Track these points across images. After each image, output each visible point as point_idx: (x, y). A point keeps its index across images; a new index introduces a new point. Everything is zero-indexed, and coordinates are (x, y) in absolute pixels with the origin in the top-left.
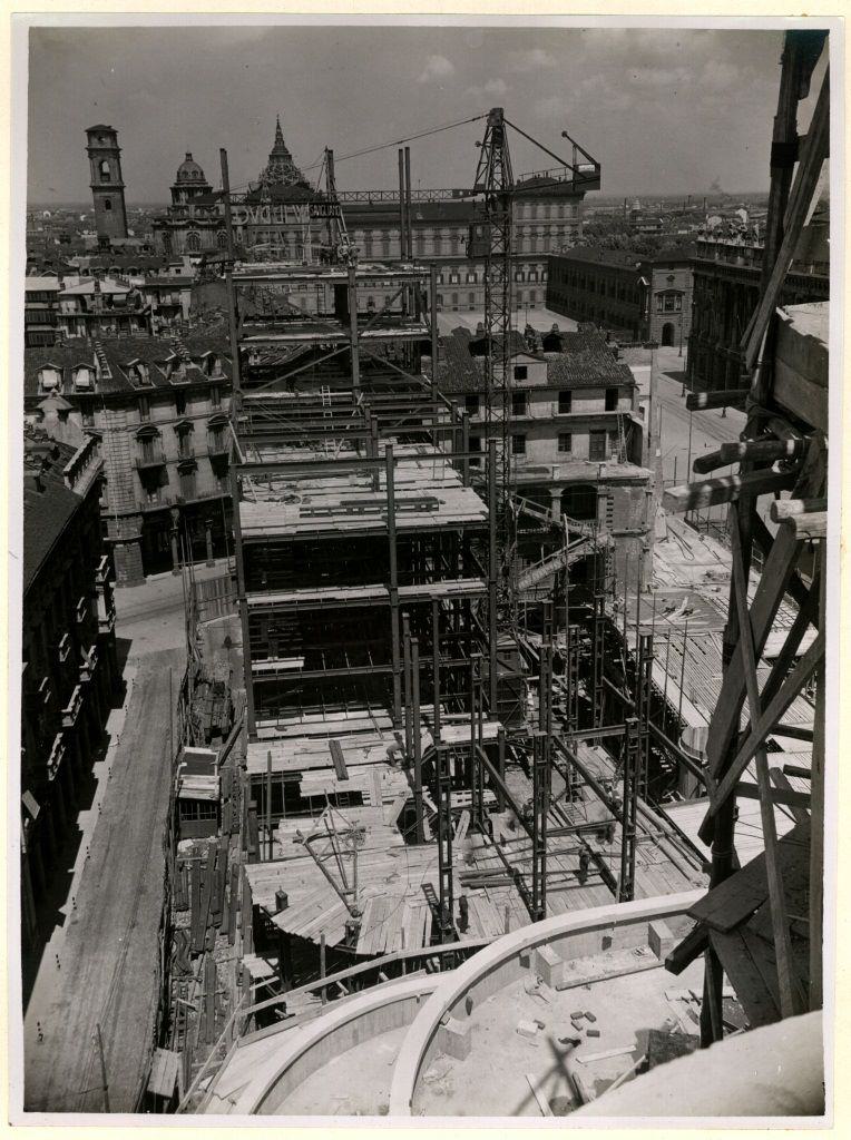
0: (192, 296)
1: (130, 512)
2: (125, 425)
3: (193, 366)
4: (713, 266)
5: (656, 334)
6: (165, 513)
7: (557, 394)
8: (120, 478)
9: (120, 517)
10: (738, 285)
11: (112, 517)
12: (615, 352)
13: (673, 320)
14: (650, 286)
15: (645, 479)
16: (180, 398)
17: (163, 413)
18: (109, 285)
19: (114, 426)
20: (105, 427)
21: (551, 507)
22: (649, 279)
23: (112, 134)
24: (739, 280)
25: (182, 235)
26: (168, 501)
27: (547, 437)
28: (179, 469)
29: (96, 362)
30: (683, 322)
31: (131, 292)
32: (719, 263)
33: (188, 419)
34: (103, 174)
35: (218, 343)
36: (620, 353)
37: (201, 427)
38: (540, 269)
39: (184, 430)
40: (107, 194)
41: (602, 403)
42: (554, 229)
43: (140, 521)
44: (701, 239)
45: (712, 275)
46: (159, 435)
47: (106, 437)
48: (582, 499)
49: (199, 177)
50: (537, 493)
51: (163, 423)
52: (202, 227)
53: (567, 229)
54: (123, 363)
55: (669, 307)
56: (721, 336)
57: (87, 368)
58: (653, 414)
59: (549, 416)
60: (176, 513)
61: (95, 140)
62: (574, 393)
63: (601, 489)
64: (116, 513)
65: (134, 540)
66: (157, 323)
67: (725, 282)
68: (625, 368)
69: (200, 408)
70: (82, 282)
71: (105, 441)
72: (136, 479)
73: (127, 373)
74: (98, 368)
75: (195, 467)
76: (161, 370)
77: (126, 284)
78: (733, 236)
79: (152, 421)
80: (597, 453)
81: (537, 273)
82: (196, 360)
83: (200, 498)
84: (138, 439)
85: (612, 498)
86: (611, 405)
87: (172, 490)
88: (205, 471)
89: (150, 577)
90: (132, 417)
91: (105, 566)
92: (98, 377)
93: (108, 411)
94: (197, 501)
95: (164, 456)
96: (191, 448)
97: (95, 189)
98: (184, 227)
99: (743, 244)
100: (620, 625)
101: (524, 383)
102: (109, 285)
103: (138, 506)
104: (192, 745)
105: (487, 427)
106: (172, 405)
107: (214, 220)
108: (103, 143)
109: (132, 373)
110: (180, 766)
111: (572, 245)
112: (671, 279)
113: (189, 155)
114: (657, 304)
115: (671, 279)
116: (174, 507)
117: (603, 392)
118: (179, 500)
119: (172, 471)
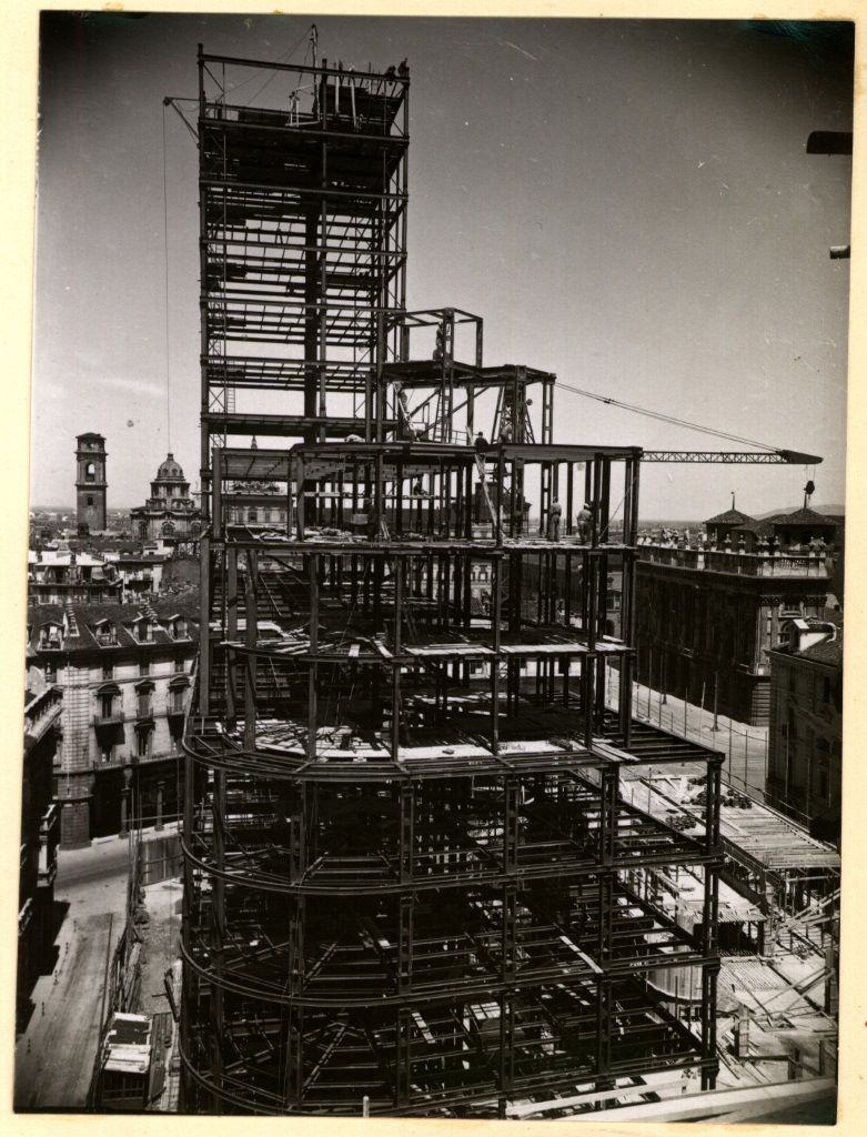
0: (163, 572)
1: (85, 769)
2: (86, 682)
3: (160, 628)
6: (116, 774)
8: (76, 735)
9: (72, 775)
11: (64, 776)
16: (144, 657)
17: (124, 672)
18: (84, 559)
19: (76, 683)
20: (67, 683)
23: (100, 440)
25: (158, 525)
26: (122, 760)
28: (136, 728)
29: (65, 622)
31: (106, 565)
32: (655, 564)
33: (151, 679)
34: (88, 475)
35: (184, 608)
37: (162, 687)
39: (145, 689)
40: (91, 492)
43: (91, 780)
45: (648, 575)
46: (120, 693)
47: (67, 694)
49: (178, 474)
51: (125, 681)
52: (177, 518)
54: (92, 623)
57: (55, 625)
60: (128, 773)
61: (84, 447)
64: (68, 771)
65: (83, 800)
66: (127, 596)
69: (163, 669)
70: (58, 556)
71: (65, 697)
72: (93, 736)
73: (95, 632)
74: (67, 627)
75: (153, 726)
76: (129, 631)
77: (102, 559)
78: (665, 541)
81: (486, 573)
82: (165, 623)
83: (155, 757)
84: (98, 697)
87: (127, 749)
88: (162, 727)
89: (96, 840)
90: (95, 675)
91: (52, 814)
92: (65, 635)
93: (71, 668)
94: (150, 760)
95: (122, 715)
96: (150, 708)
97: (80, 488)
98: (161, 517)
99: (675, 547)
102: (84, 559)
103: (91, 765)
104: (123, 1011)
106: (136, 664)
107: (189, 511)
108: (91, 449)
109: (99, 632)
110: (109, 1034)
113: (170, 456)
116: (128, 767)
118: (134, 759)
119: (128, 730)
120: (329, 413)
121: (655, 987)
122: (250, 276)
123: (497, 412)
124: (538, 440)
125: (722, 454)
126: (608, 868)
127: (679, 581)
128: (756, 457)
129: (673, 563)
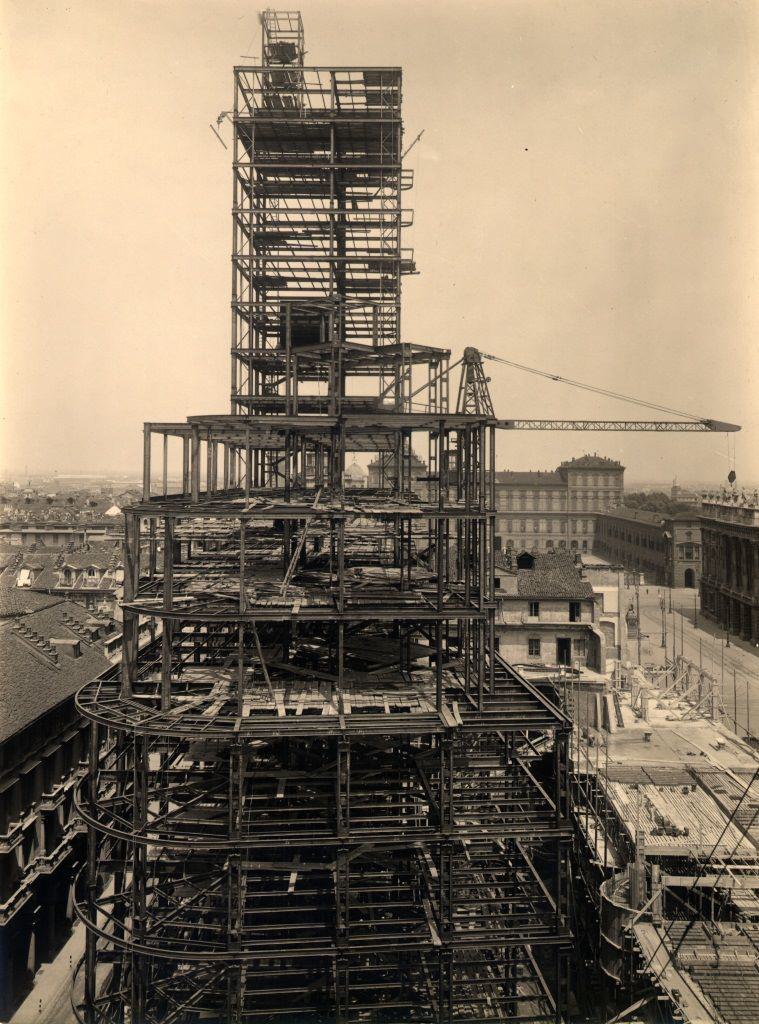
4: (714, 523)
5: (679, 576)
10: (744, 540)
12: (580, 571)
13: (693, 566)
14: (672, 539)
15: (602, 685)
22: (672, 532)
24: (735, 534)
27: (518, 643)
30: (697, 567)
32: (717, 520)
36: (585, 572)
38: (591, 527)
41: (567, 615)
42: (601, 494)
44: (706, 501)
53: (612, 494)
55: (689, 555)
56: (725, 580)
58: (622, 629)
59: (519, 623)
62: (541, 606)
67: (723, 536)
68: (588, 586)
80: (563, 655)
86: (574, 612)
111: (615, 506)
112: (689, 534)
114: (677, 553)
115: (689, 534)
117: (567, 605)
120: (300, 394)
121: (608, 940)
122: (290, 284)
123: (461, 388)
124: (408, 411)
125: (655, 423)
126: (447, 837)
127: (741, 536)
128: (684, 426)
129: (732, 521)
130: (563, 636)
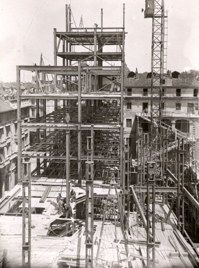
7: (175, 90)
21: (171, 126)
48: (182, 124)
50: (167, 121)
62: (182, 90)
63: (191, 122)
79: (60, 105)
85: (195, 125)
100: (194, 171)
101: (164, 85)
105: (152, 99)
130: (191, 102)
